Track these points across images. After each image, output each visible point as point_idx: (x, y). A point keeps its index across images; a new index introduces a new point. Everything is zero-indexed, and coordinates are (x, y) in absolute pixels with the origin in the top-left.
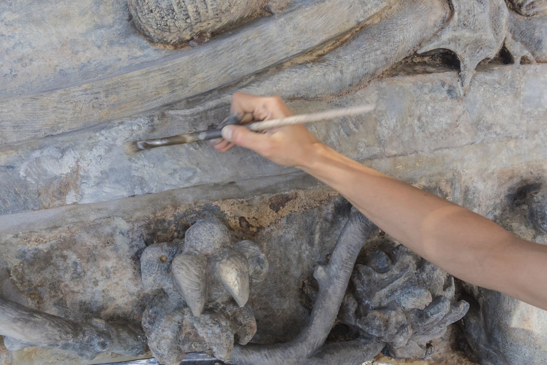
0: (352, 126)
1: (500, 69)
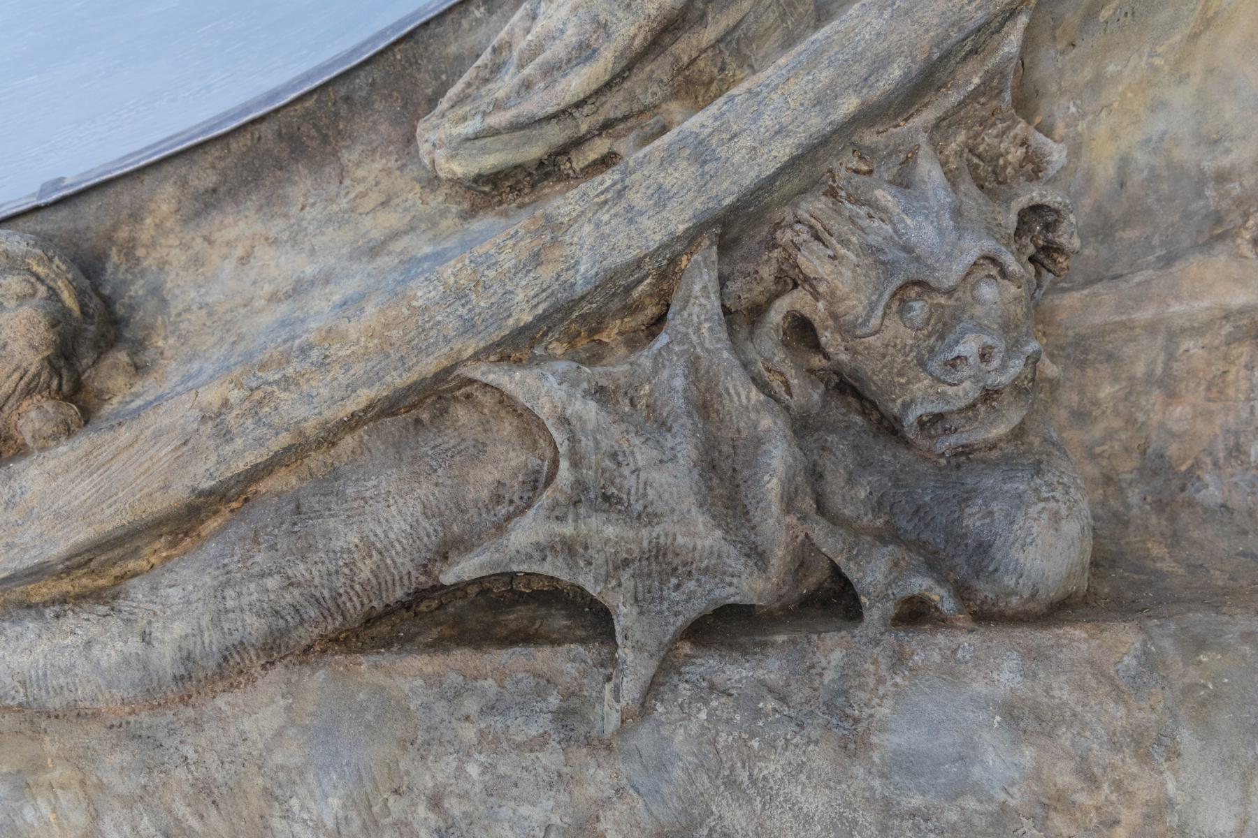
0: (181, 809)
1: (794, 642)
